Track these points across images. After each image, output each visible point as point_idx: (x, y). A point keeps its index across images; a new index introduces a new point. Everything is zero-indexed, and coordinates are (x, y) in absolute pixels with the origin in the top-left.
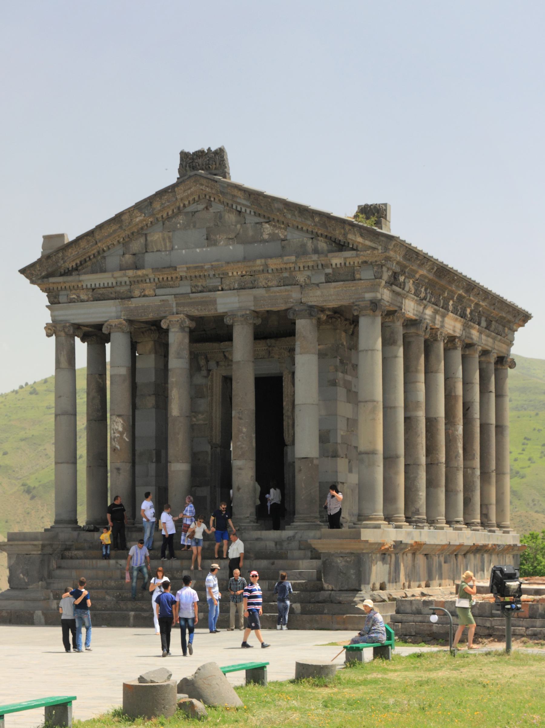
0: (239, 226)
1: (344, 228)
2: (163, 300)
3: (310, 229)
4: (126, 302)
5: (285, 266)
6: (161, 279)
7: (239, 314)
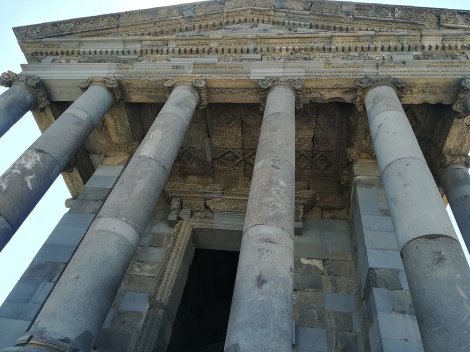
1: (439, 18)
2: (177, 67)
5: (353, 45)
6: (183, 49)
7: (282, 79)
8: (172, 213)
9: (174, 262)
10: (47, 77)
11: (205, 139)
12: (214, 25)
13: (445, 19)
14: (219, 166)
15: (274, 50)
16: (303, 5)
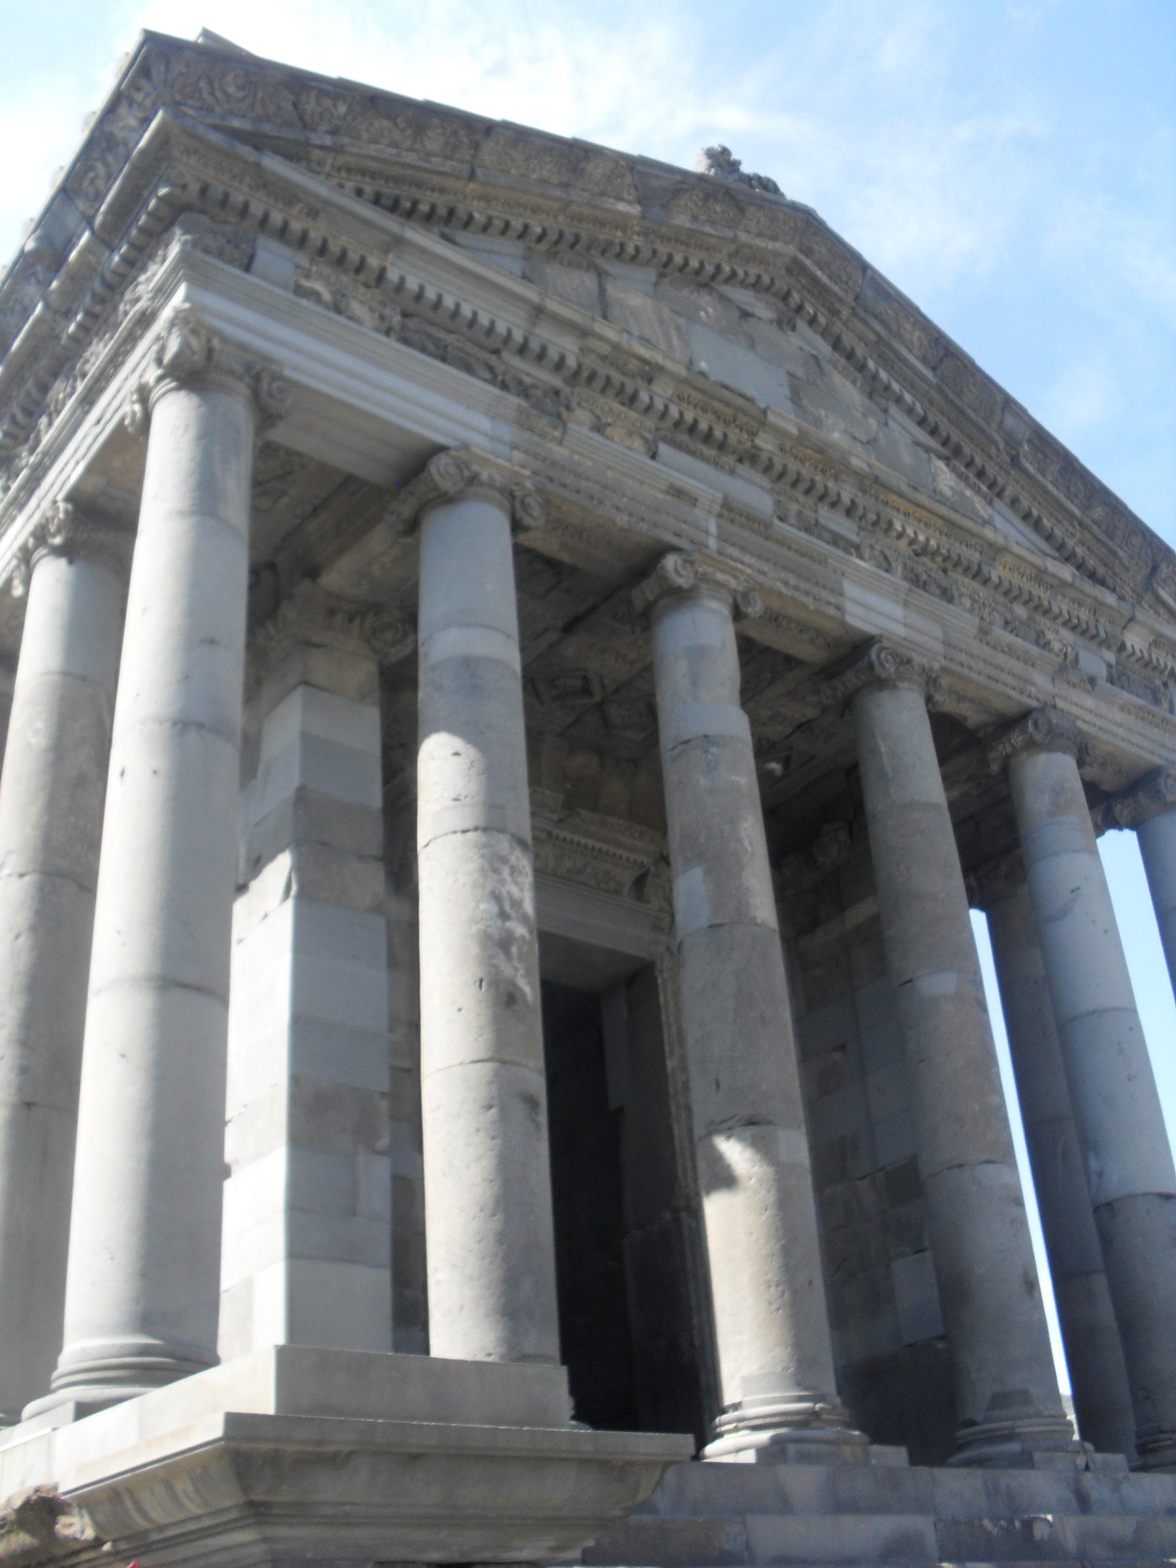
0: (872, 422)
1: (1154, 570)
2: (677, 493)
3: (1058, 532)
4: (543, 423)
5: (1027, 586)
6: (689, 417)
10: (296, 368)
12: (699, 271)
13: (1164, 576)
15: (890, 524)
16: (926, 343)
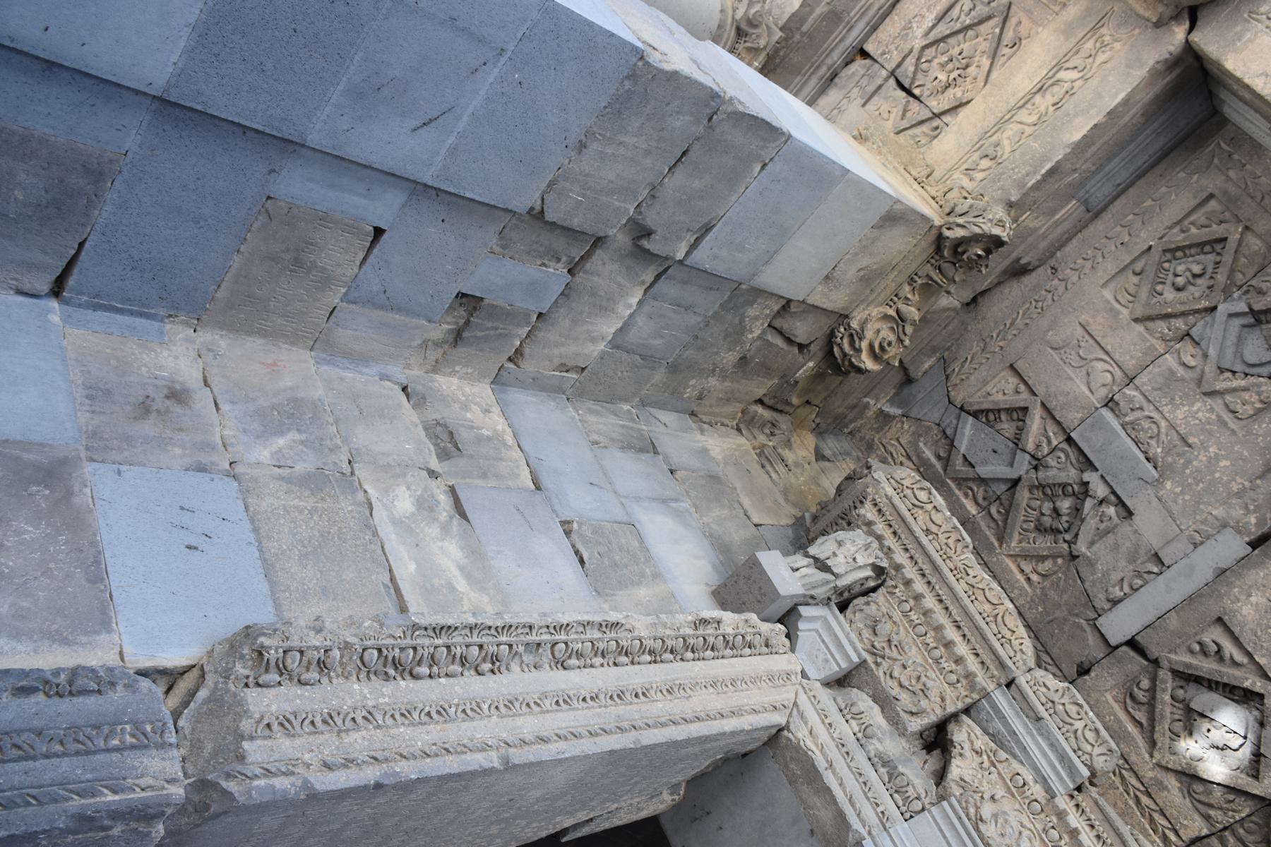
8: (799, 560)
9: (563, 701)
11: (1229, 534)
14: (1109, 697)
